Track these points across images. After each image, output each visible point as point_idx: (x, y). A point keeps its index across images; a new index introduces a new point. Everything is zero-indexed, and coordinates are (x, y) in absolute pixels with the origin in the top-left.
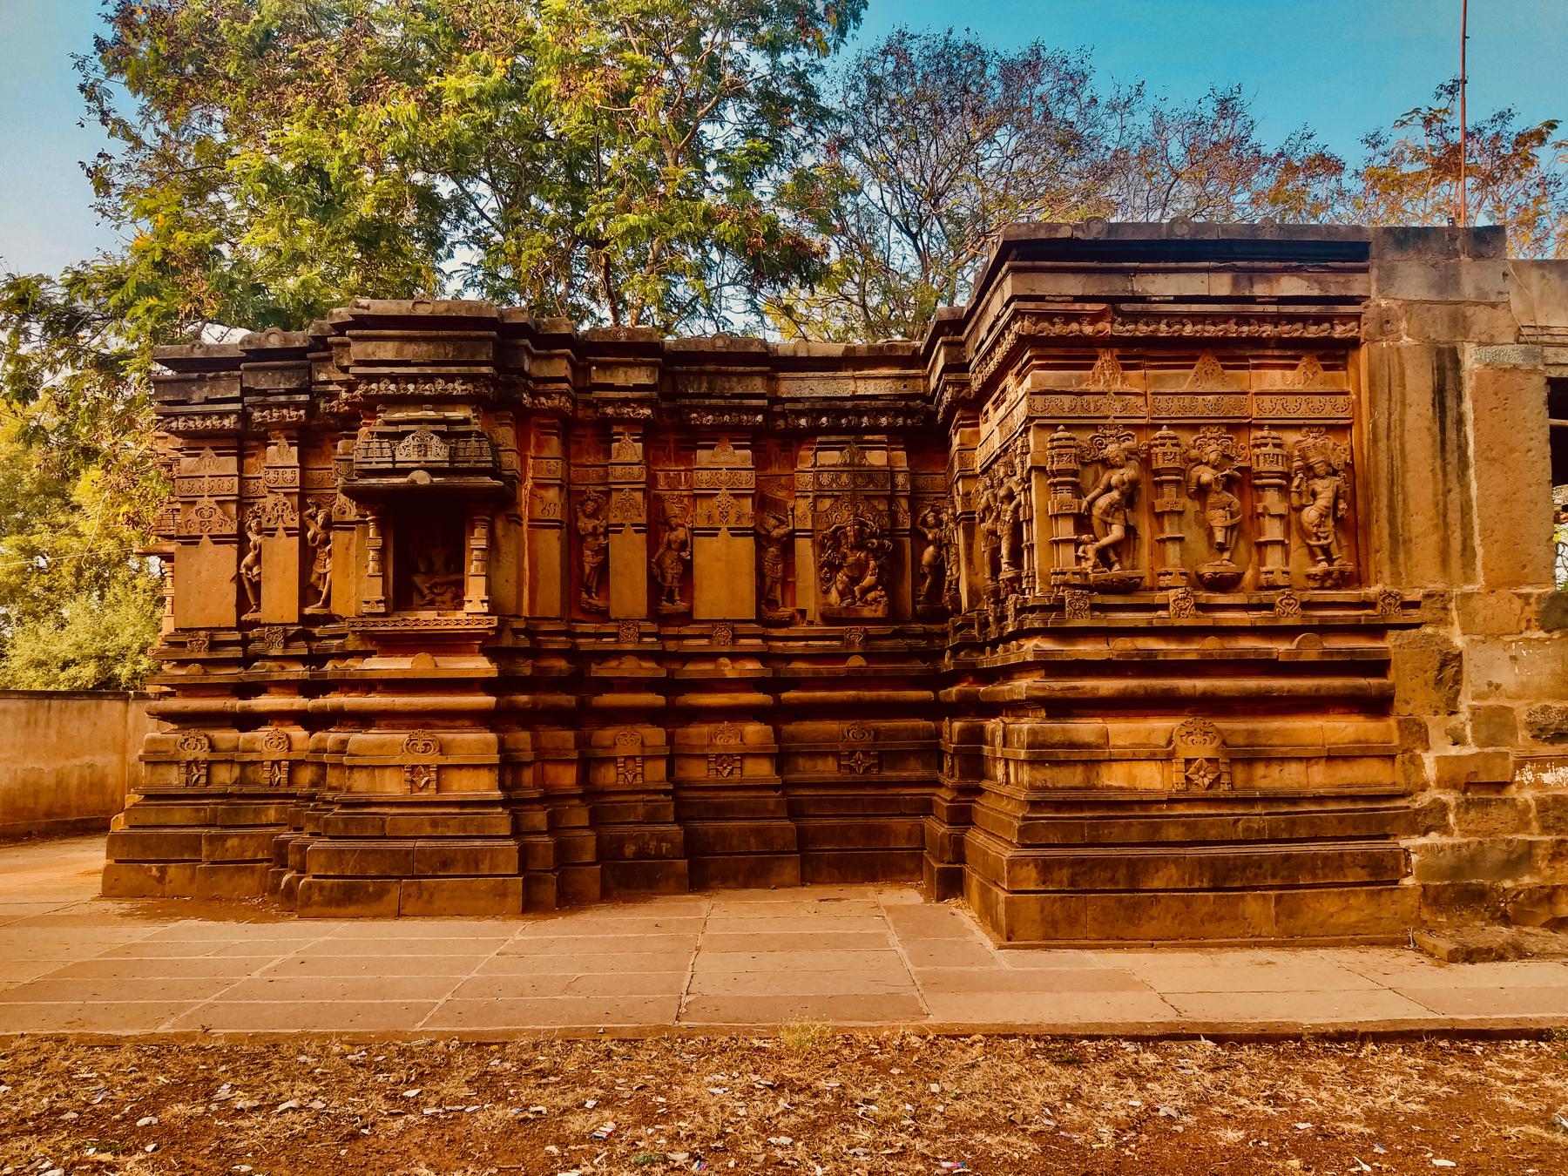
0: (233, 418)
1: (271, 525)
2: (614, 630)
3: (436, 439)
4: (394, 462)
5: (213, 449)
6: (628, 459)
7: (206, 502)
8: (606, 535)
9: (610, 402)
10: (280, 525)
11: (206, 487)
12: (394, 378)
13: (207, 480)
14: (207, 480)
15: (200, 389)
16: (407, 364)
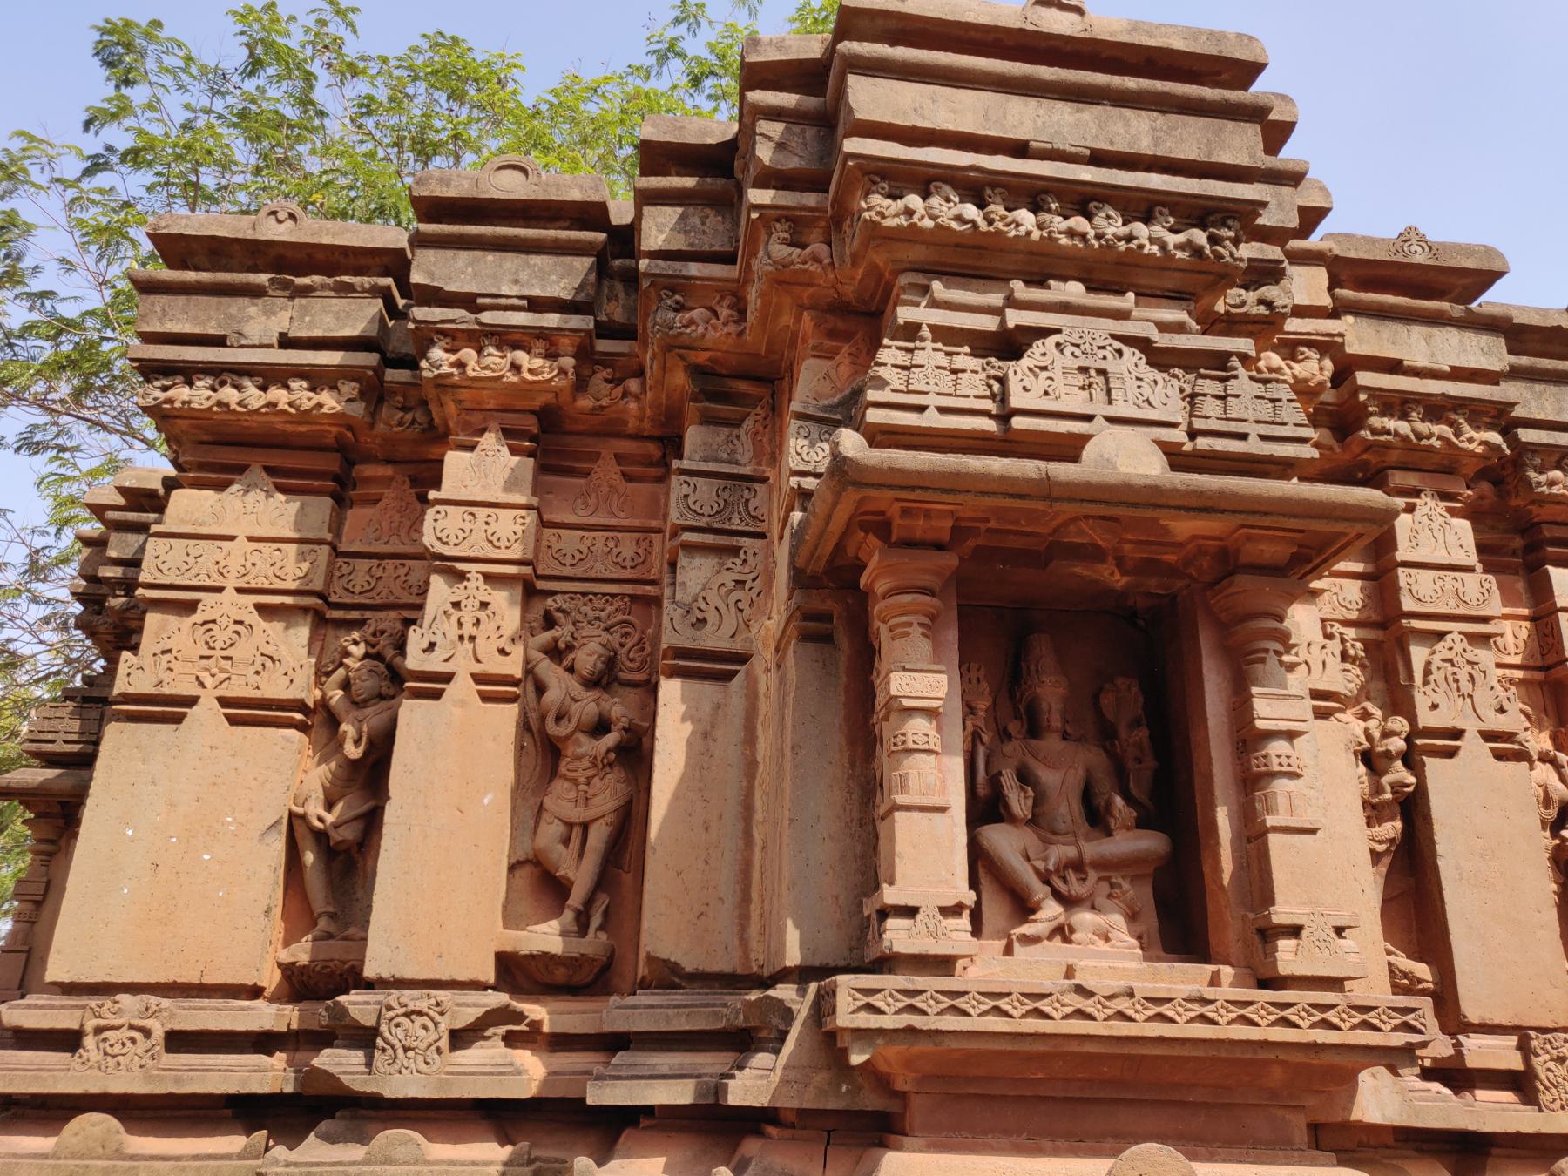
0: (350, 388)
1: (434, 663)
2: (1515, 1062)
3: (1132, 356)
4: (1005, 416)
5: (270, 471)
6: (1441, 557)
7: (227, 606)
8: (1410, 759)
9: (1399, 404)
10: (463, 667)
11: (234, 564)
12: (975, 188)
13: (241, 546)
14: (241, 546)
15: (269, 313)
16: (1020, 149)
